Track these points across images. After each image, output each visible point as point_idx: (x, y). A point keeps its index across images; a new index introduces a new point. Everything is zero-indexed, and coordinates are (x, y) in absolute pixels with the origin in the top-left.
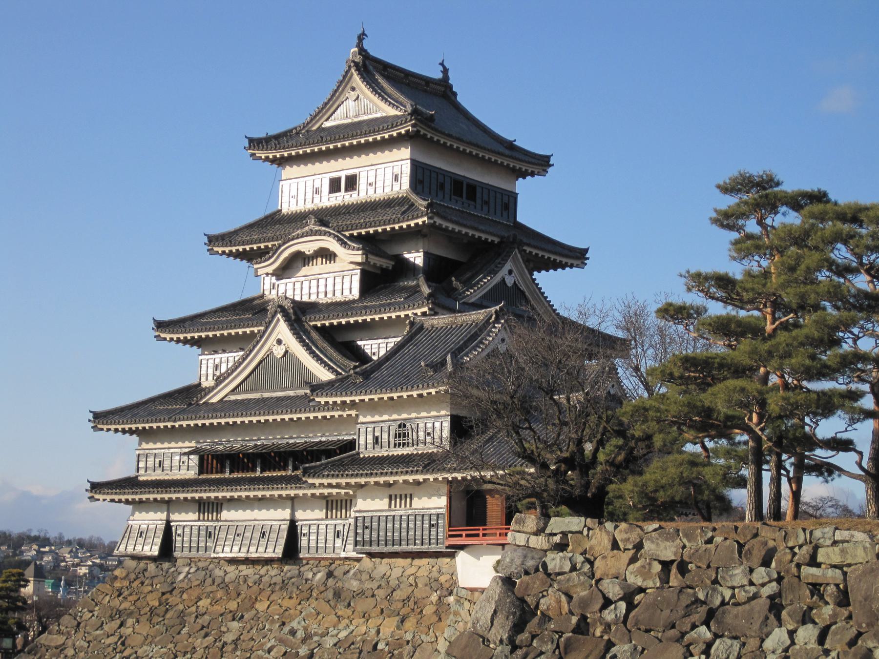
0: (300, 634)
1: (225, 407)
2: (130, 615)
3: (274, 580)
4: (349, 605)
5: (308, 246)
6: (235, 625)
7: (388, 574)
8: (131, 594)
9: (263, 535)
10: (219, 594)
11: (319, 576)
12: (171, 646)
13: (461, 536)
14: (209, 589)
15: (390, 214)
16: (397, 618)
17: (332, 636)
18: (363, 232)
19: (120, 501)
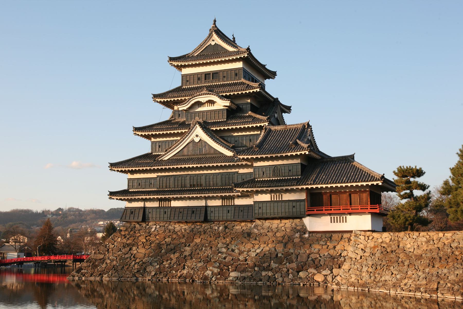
0: (237, 251)
1: (170, 161)
2: (133, 245)
3: (199, 230)
4: (256, 239)
5: (203, 99)
6: (187, 248)
7: (271, 226)
8: (131, 237)
9: (193, 212)
10: (174, 236)
11: (221, 228)
12: (159, 257)
13: (314, 210)
14: (168, 234)
15: (239, 87)
16: (282, 244)
17: (253, 252)
18: (228, 94)
19: (124, 200)
